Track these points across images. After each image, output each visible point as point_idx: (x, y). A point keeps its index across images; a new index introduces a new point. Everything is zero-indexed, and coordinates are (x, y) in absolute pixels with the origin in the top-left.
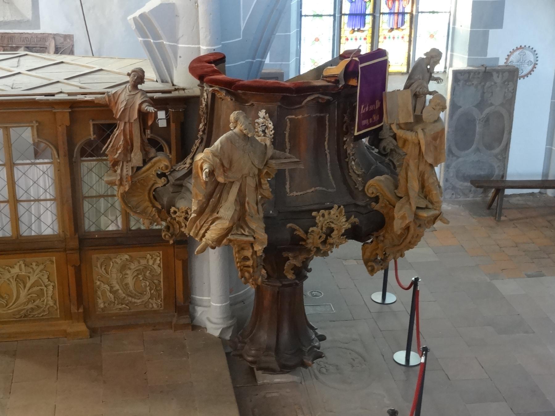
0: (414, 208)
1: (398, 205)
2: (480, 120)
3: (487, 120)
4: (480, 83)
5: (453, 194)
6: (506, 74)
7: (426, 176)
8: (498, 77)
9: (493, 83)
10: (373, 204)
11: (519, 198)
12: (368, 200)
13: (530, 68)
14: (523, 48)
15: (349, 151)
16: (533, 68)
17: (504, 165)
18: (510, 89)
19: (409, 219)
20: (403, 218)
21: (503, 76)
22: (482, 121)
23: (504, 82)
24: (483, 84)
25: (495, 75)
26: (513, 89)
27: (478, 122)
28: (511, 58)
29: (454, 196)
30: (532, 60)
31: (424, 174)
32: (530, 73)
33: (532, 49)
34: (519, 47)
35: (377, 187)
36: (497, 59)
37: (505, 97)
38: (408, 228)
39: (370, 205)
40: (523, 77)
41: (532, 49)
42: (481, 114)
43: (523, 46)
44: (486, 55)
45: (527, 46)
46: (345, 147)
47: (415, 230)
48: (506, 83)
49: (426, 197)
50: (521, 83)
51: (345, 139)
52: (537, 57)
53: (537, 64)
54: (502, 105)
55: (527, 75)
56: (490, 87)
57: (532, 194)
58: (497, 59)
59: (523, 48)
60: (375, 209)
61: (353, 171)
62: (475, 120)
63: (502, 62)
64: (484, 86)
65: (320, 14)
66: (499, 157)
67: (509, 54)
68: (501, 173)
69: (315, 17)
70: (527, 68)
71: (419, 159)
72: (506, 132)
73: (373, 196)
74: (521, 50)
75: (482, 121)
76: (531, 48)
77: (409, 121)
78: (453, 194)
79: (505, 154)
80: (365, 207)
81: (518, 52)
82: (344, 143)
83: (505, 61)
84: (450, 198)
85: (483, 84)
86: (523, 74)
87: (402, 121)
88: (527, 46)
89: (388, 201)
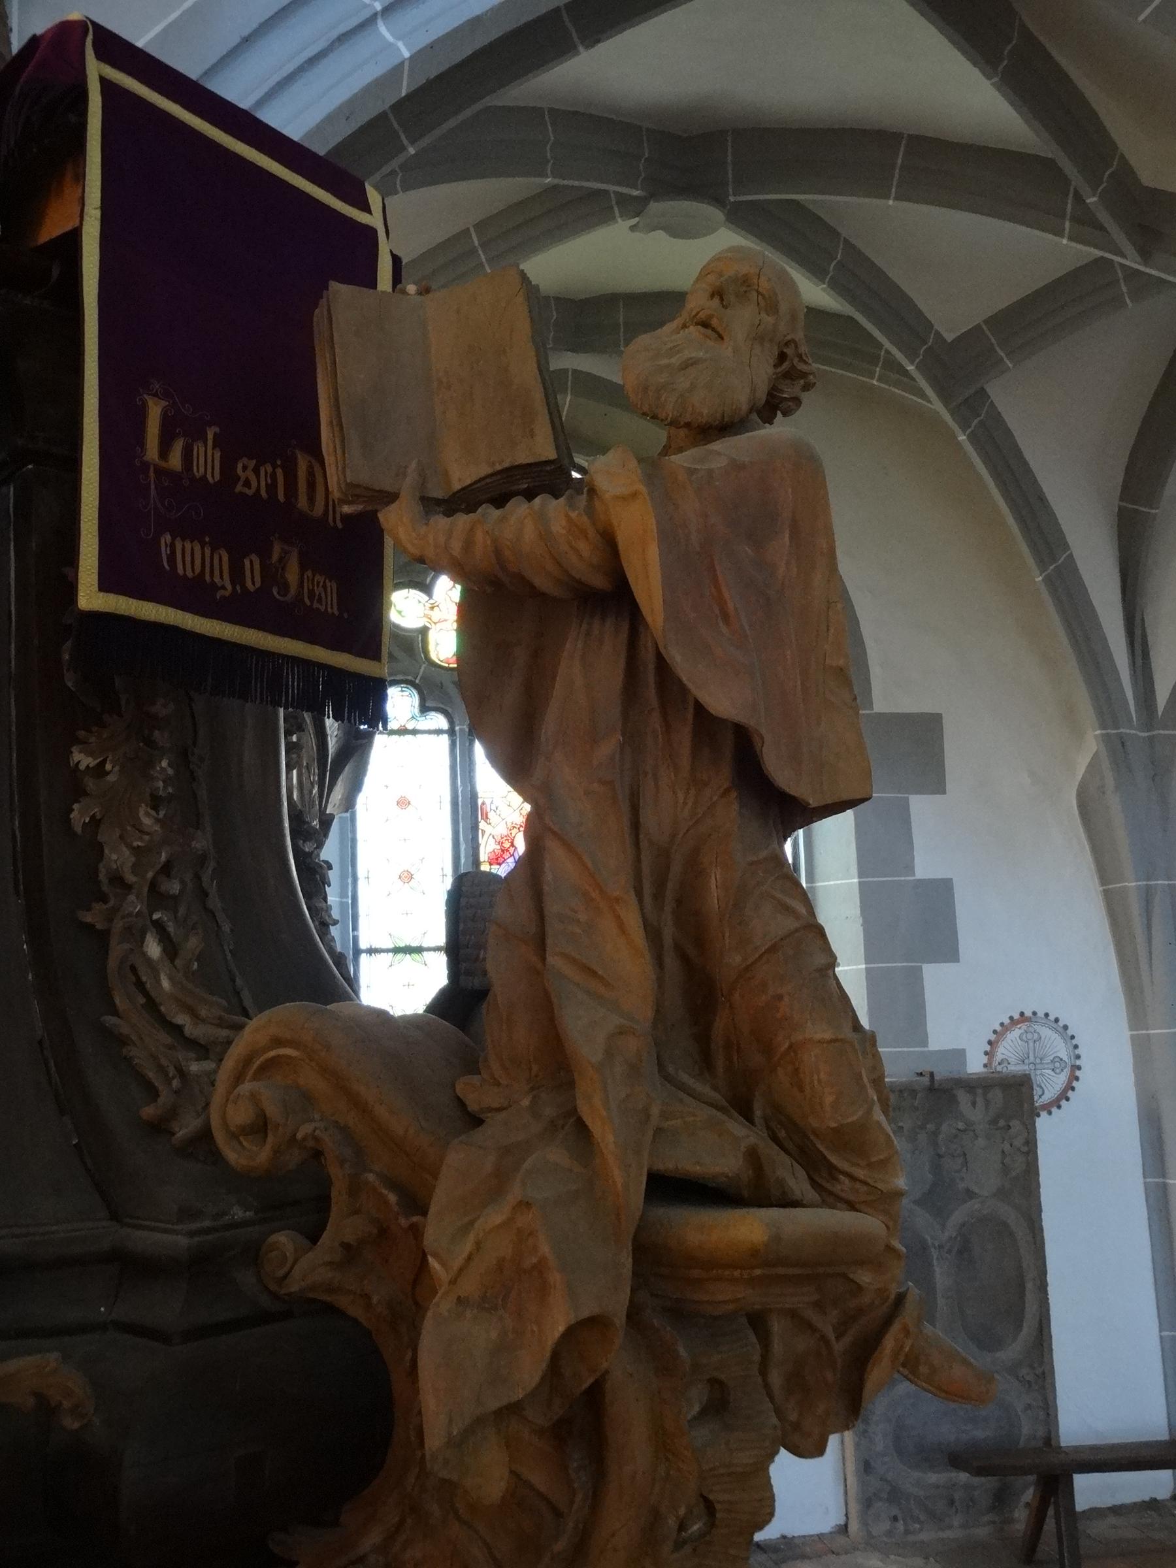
0: (626, 1183)
1: (461, 1164)
2: (941, 1247)
3: (963, 1251)
4: (923, 1127)
5: (895, 1519)
6: (997, 1096)
7: (715, 890)
8: (974, 1104)
9: (961, 1125)
10: (284, 1240)
11: (1112, 1520)
12: (238, 1213)
13: (1061, 1079)
14: (1029, 1020)
15: (118, 857)
16: (1070, 1082)
17: (1045, 1400)
18: (1018, 1142)
19: (588, 1285)
20: (513, 1284)
21: (987, 1103)
22: (949, 1252)
23: (994, 1122)
24: (931, 1127)
25: (963, 1098)
26: (1027, 1143)
27: (935, 1253)
28: (1001, 1052)
29: (900, 1526)
30: (1063, 1054)
31: (695, 871)
32: (1064, 1096)
33: (1057, 1020)
34: (1016, 1016)
35: (310, 1079)
36: (960, 1054)
37: (1005, 1170)
38: (577, 1420)
39: (253, 1253)
40: (1048, 1108)
41: (1057, 1020)
42: (943, 1226)
43: (1028, 1013)
44: (924, 1042)
45: (1041, 1014)
46: (79, 816)
47: (663, 1443)
48: (1002, 1123)
49: (744, 1109)
50: (1043, 1123)
51: (82, 759)
52: (1076, 1047)
53: (1079, 1068)
54: (1002, 1194)
55: (1057, 1103)
56: (956, 1136)
57: (1152, 1505)
58: (960, 1054)
59: (1029, 1020)
60: (294, 1286)
61: (152, 1005)
62: (925, 1248)
63: (975, 1065)
64: (936, 1133)
65: (414, 944)
66: (1024, 1371)
67: (993, 1037)
68: (1041, 1432)
69: (400, 956)
70: (1049, 1084)
71: (632, 739)
72: (1029, 1286)
73: (260, 1155)
74: (1024, 1026)
75: (949, 1252)
76: (1052, 1018)
77: (523, 458)
78: (895, 1519)
79: (1041, 1363)
80: (203, 1266)
81: (1015, 1033)
82: (75, 786)
83: (985, 1059)
84: (890, 1533)
85: (931, 1127)
86: (1048, 1096)
87: (462, 475)
88: (1041, 1014)
89: (394, 1185)
